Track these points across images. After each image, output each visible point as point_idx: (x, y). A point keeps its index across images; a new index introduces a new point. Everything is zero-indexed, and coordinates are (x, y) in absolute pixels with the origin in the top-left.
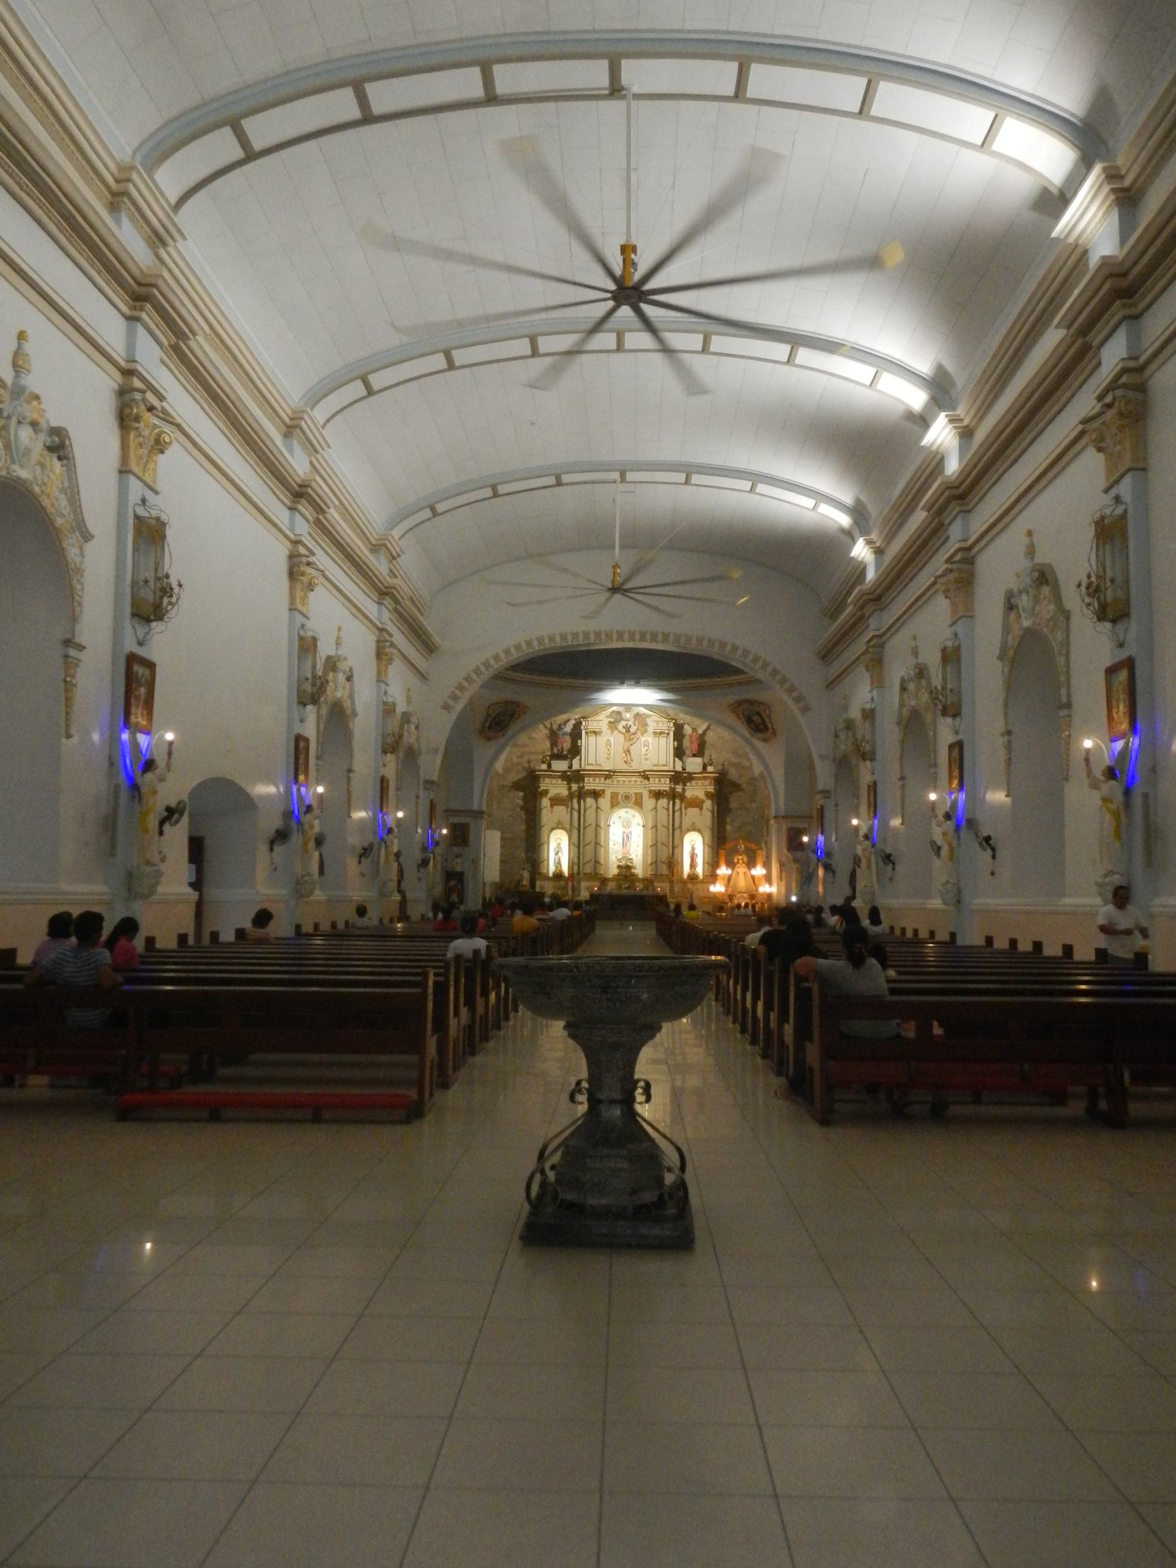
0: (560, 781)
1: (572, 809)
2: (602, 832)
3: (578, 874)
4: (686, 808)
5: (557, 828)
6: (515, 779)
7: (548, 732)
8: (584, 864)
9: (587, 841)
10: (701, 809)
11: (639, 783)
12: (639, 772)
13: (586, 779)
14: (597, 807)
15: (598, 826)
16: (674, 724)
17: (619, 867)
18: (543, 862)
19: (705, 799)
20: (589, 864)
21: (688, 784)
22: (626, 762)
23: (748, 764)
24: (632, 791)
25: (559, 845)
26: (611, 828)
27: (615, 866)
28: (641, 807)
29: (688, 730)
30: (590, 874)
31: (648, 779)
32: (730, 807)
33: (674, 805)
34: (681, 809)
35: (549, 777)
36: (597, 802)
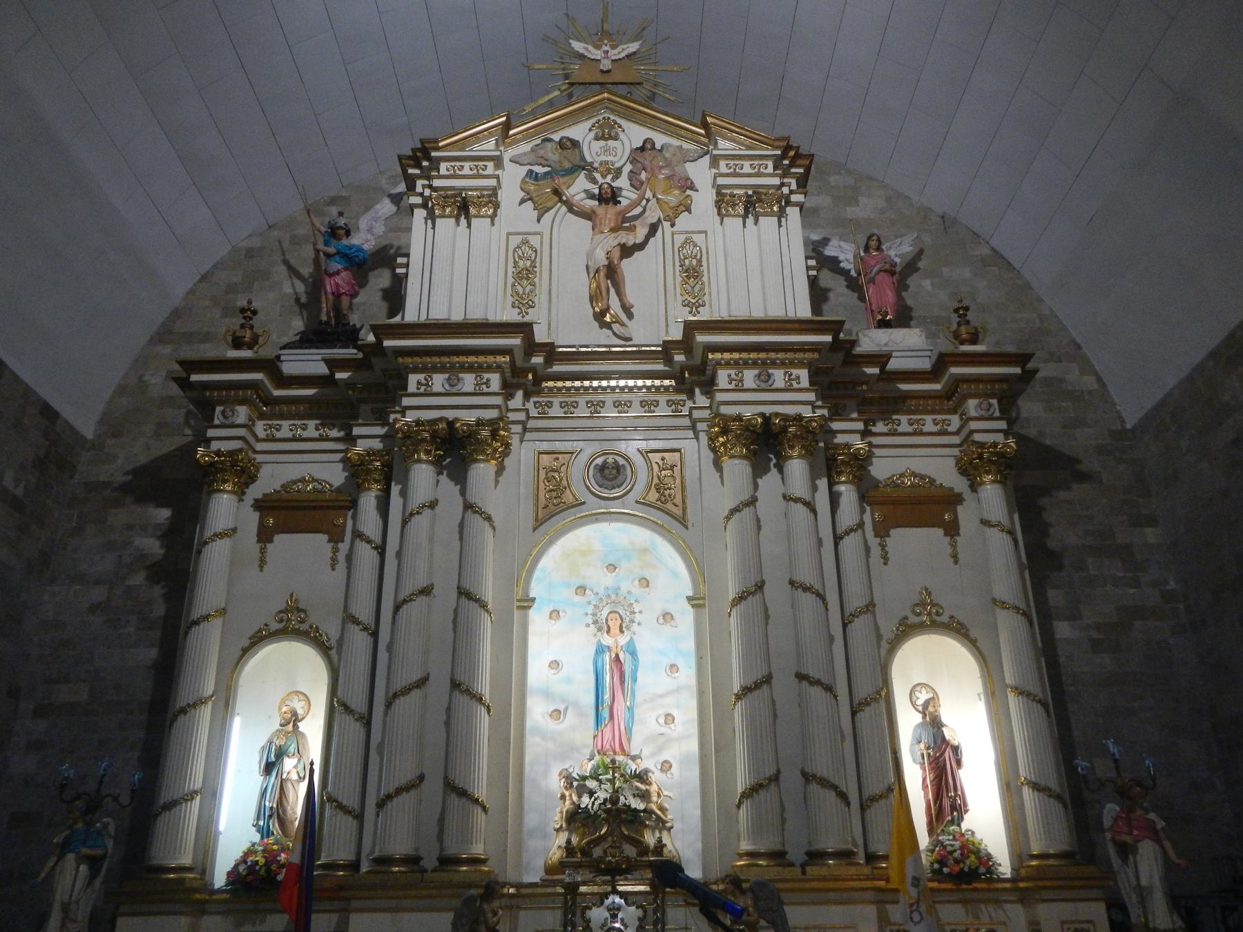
0: (311, 428)
1: (358, 535)
2: (487, 627)
3: (354, 866)
4: (882, 531)
5: (285, 632)
6: (143, 459)
7: (301, 287)
8: (381, 805)
9: (400, 682)
10: (952, 530)
11: (663, 410)
12: (668, 349)
13: (413, 379)
14: (468, 506)
15: (465, 594)
16: (803, 182)
17: (576, 818)
18: (174, 804)
19: (958, 483)
20: (404, 797)
21: (880, 427)
22: (599, 317)
23: (1089, 382)
24: (632, 447)
25: (294, 719)
26: (537, 618)
27: (557, 818)
28: (682, 521)
29: (844, 252)
30: (413, 861)
31: (709, 386)
32: (1052, 544)
33: (834, 499)
34: (861, 525)
35: (271, 408)
36: (463, 492)
